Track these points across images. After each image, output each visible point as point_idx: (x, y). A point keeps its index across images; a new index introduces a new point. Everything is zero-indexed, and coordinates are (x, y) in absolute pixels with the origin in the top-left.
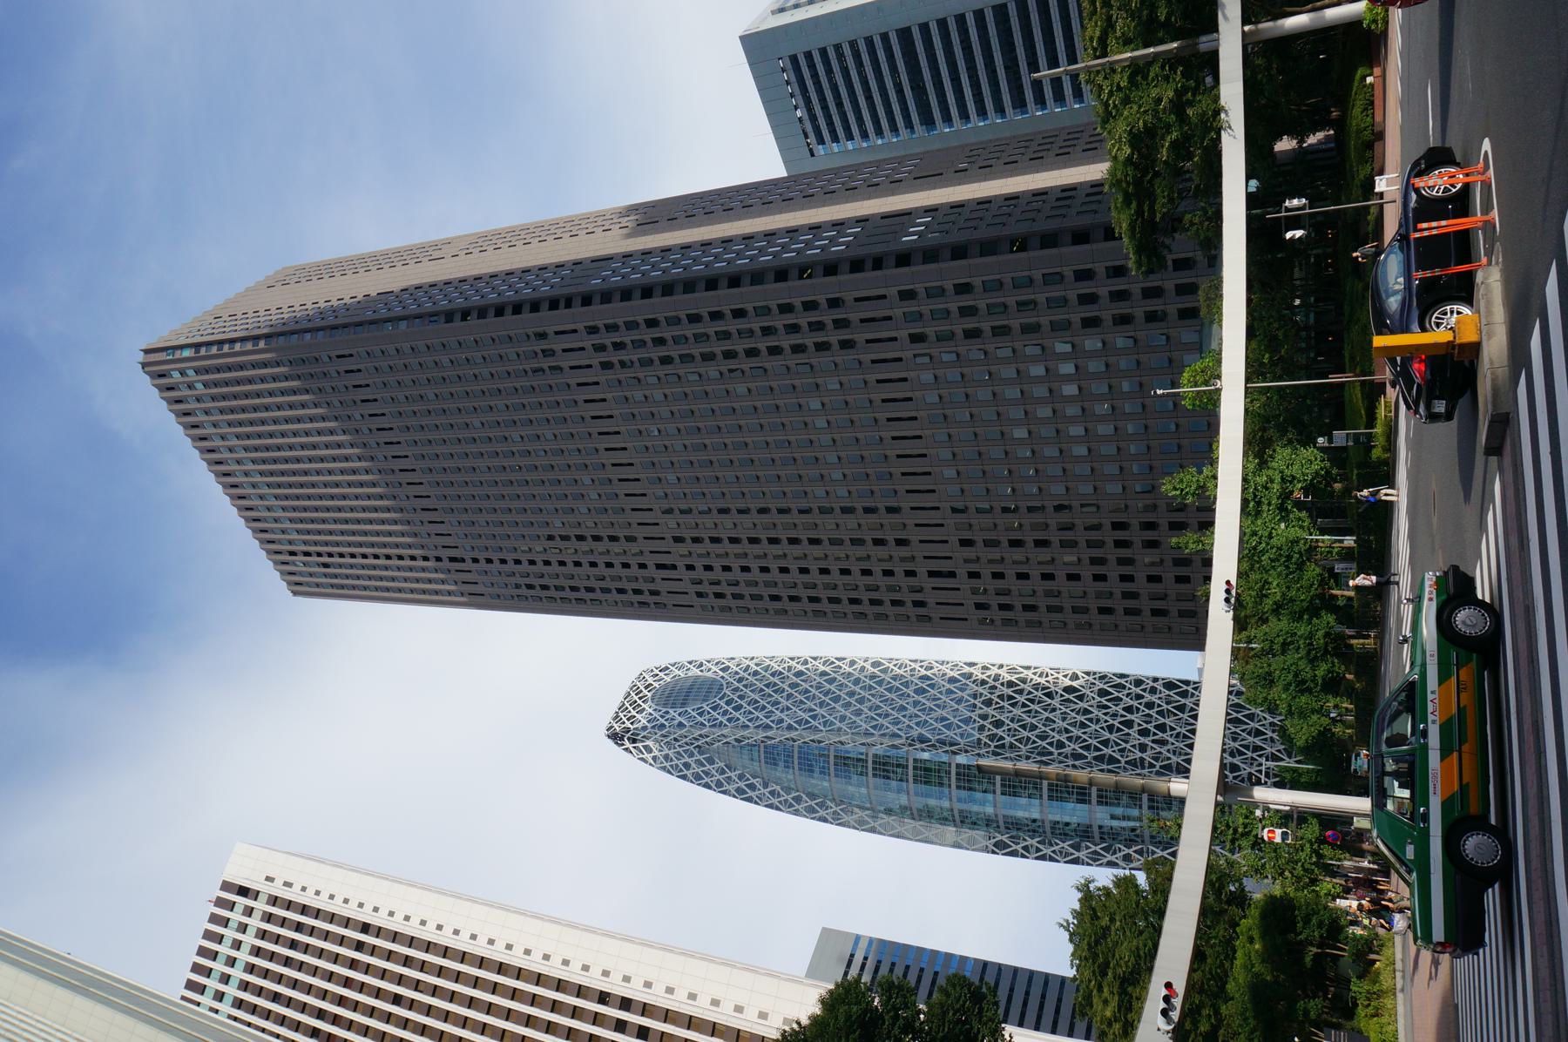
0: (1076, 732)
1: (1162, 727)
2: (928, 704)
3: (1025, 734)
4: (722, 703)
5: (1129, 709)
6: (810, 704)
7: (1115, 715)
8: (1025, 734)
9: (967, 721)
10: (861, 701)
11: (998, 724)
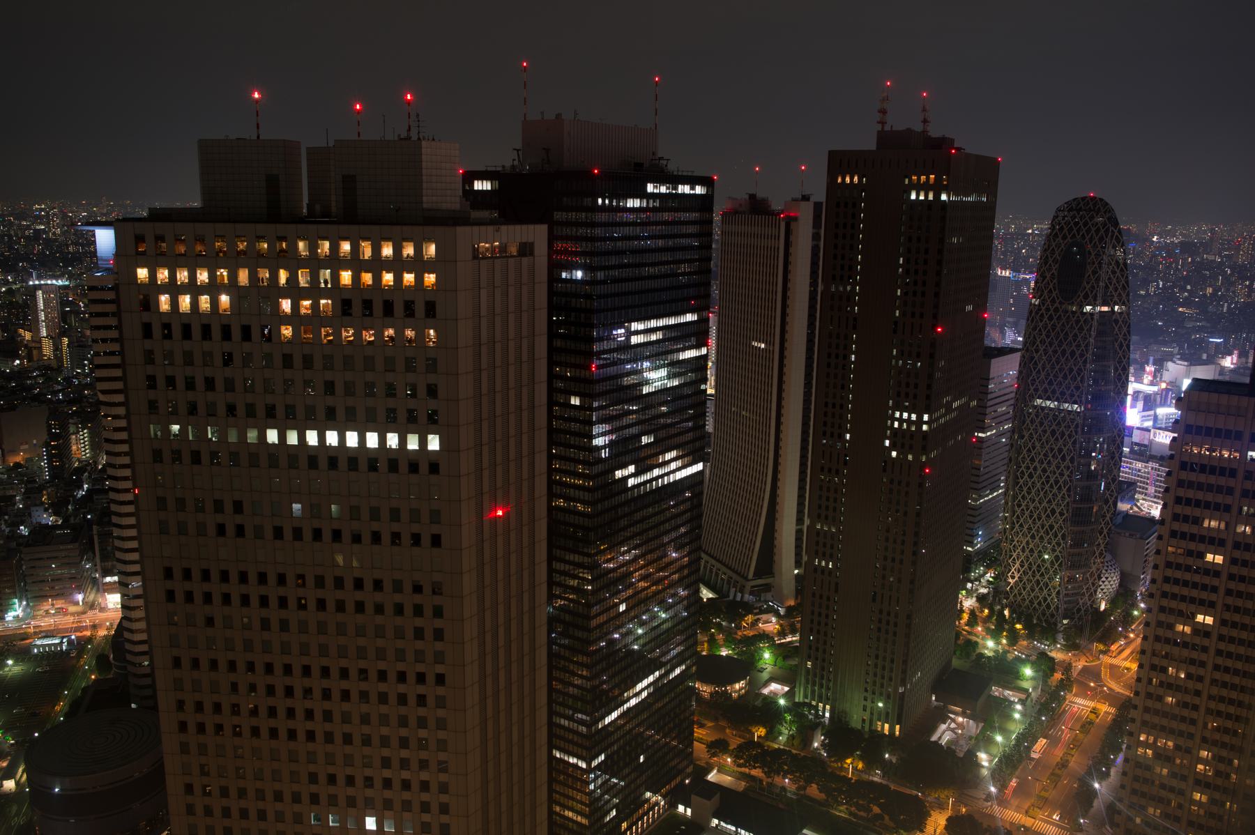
0: (1027, 513)
1: (1032, 551)
2: (1044, 439)
3: (1025, 489)
5: (1042, 538)
7: (1038, 531)
8: (1025, 489)
9: (1032, 460)
11: (1031, 476)
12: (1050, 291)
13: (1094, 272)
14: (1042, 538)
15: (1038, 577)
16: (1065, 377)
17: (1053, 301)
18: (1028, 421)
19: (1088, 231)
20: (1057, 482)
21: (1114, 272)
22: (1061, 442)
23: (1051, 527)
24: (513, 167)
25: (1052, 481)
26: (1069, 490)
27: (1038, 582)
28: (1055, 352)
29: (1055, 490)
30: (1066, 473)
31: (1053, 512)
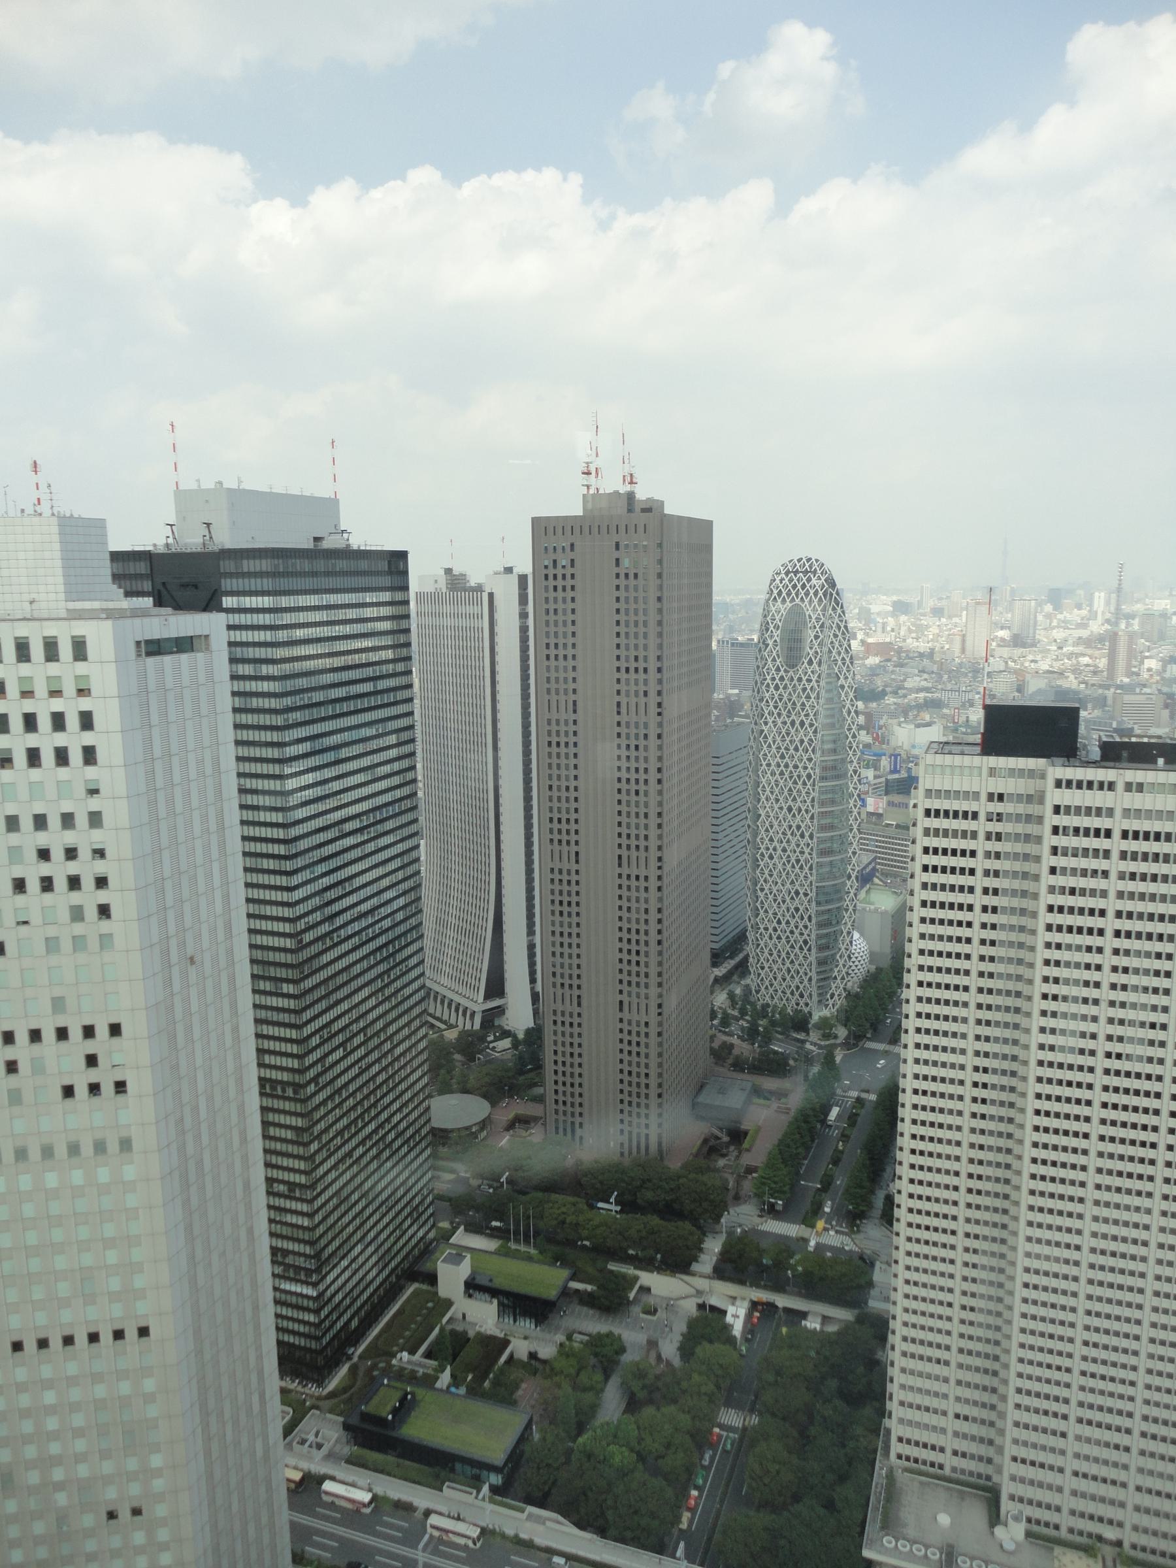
1: (779, 938)
4: (782, 673)
5: (788, 922)
6: (778, 739)
9: (771, 840)
10: (782, 773)
11: (771, 857)
12: (774, 660)
13: (816, 637)
14: (788, 922)
15: (788, 964)
16: (796, 749)
17: (778, 669)
18: (763, 798)
19: (807, 594)
20: (798, 861)
21: (836, 636)
22: (798, 818)
23: (797, 910)
24: (167, 545)
25: (793, 860)
26: (811, 869)
27: (789, 971)
28: (785, 723)
29: (797, 870)
30: (807, 851)
31: (797, 893)
